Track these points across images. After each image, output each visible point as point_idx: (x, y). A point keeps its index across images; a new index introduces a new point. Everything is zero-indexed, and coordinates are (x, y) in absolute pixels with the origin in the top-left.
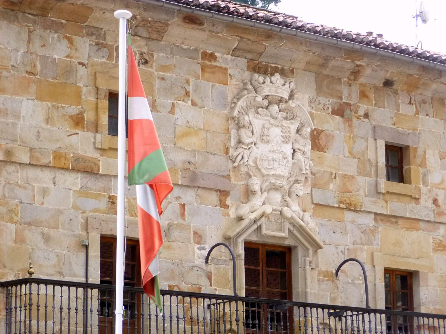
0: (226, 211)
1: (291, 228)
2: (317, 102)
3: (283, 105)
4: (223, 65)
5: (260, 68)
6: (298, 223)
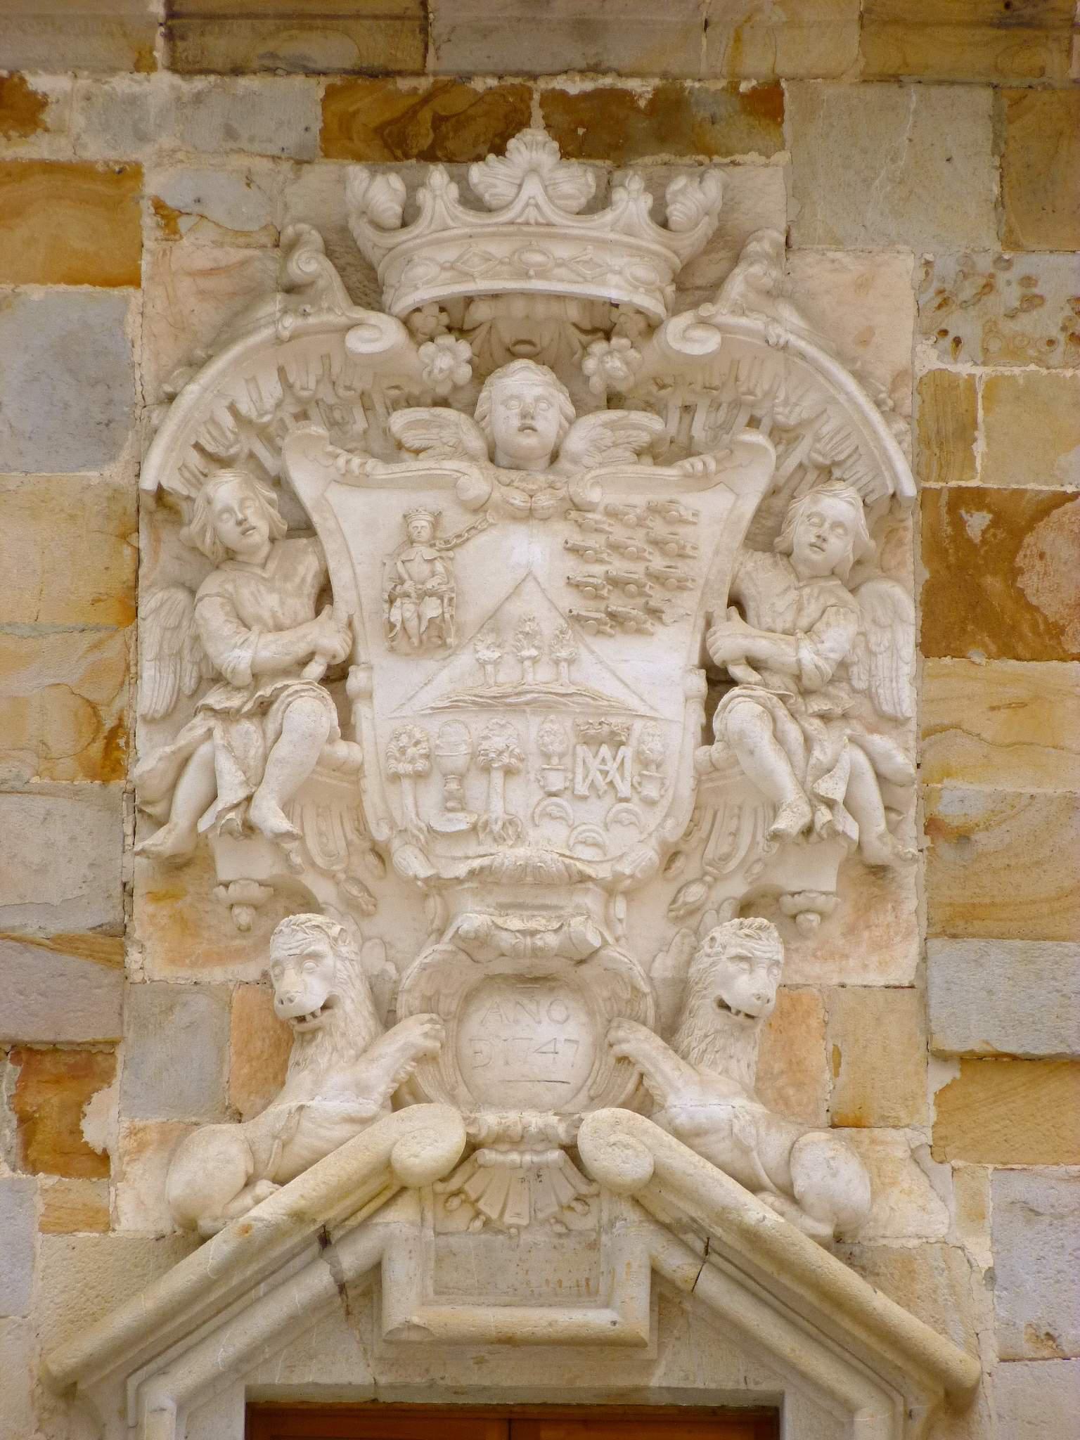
0: (79, 1190)
1: (678, 1264)
2: (1010, 295)
3: (608, 363)
4: (97, 151)
5: (443, 130)
6: (722, 1215)
